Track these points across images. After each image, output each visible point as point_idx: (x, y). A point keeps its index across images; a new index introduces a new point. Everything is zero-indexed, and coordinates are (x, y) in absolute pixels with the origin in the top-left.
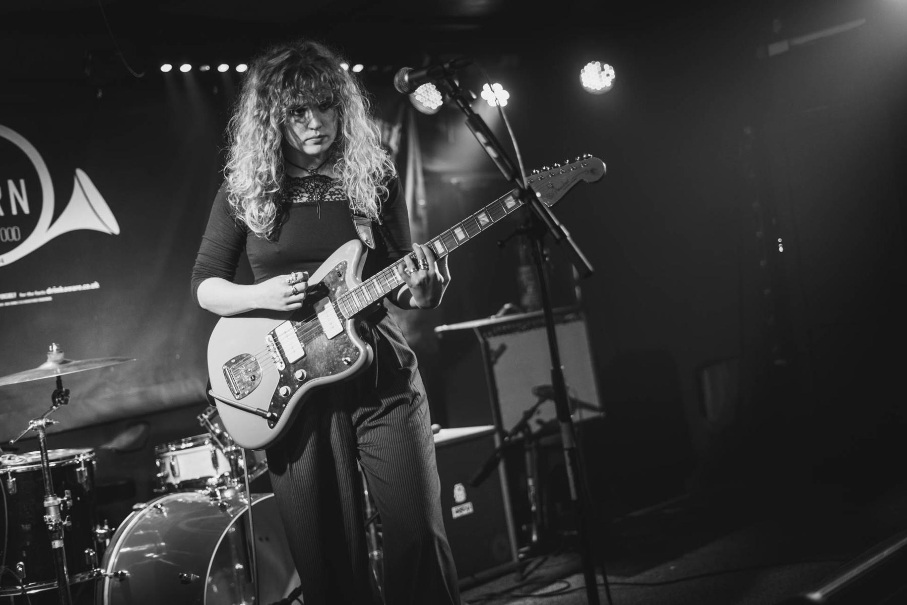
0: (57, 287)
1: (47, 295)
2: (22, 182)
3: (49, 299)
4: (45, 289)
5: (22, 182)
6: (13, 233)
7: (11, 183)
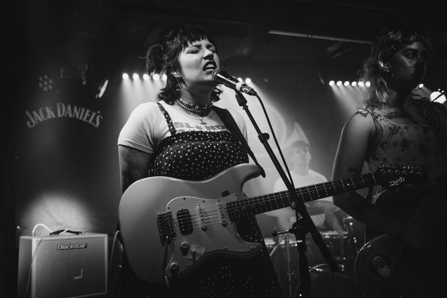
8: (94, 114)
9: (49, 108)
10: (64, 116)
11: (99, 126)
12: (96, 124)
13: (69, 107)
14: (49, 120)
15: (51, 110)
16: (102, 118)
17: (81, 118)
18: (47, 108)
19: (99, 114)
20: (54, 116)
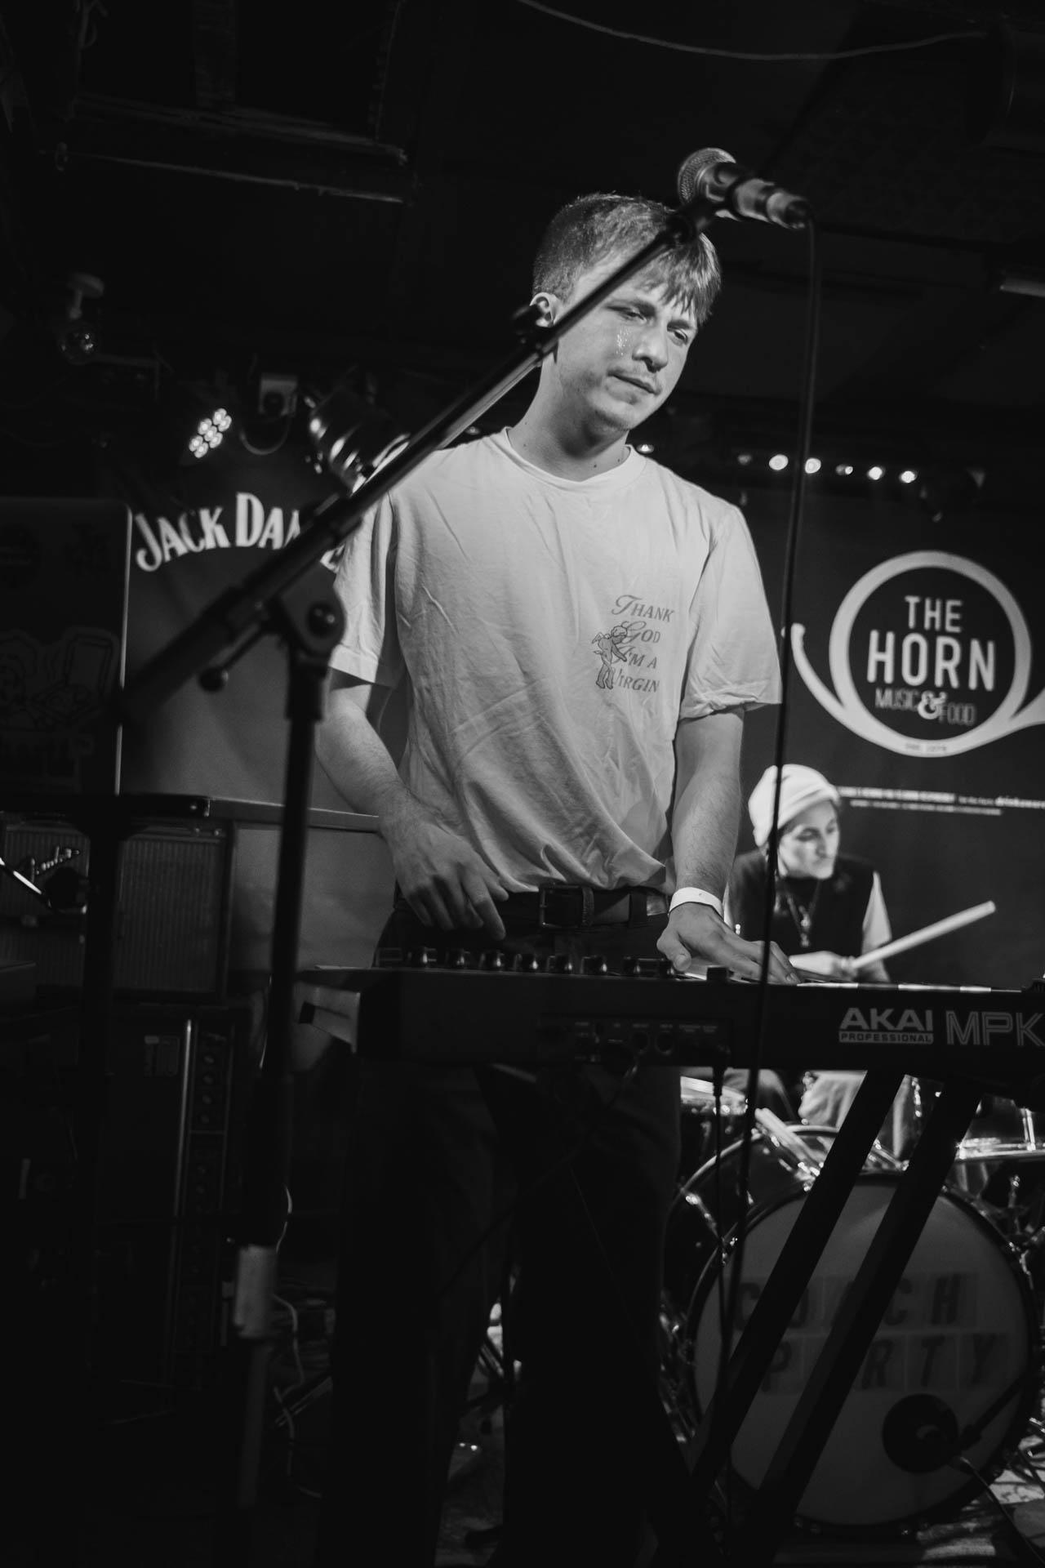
0: (1012, 797)
1: (995, 807)
2: (991, 646)
3: (997, 812)
4: (995, 797)
5: (991, 646)
6: (965, 713)
7: (975, 646)
9: (212, 514)
10: (256, 545)
13: (277, 515)
14: (205, 551)
15: (219, 522)
18: (204, 514)
20: (224, 542)
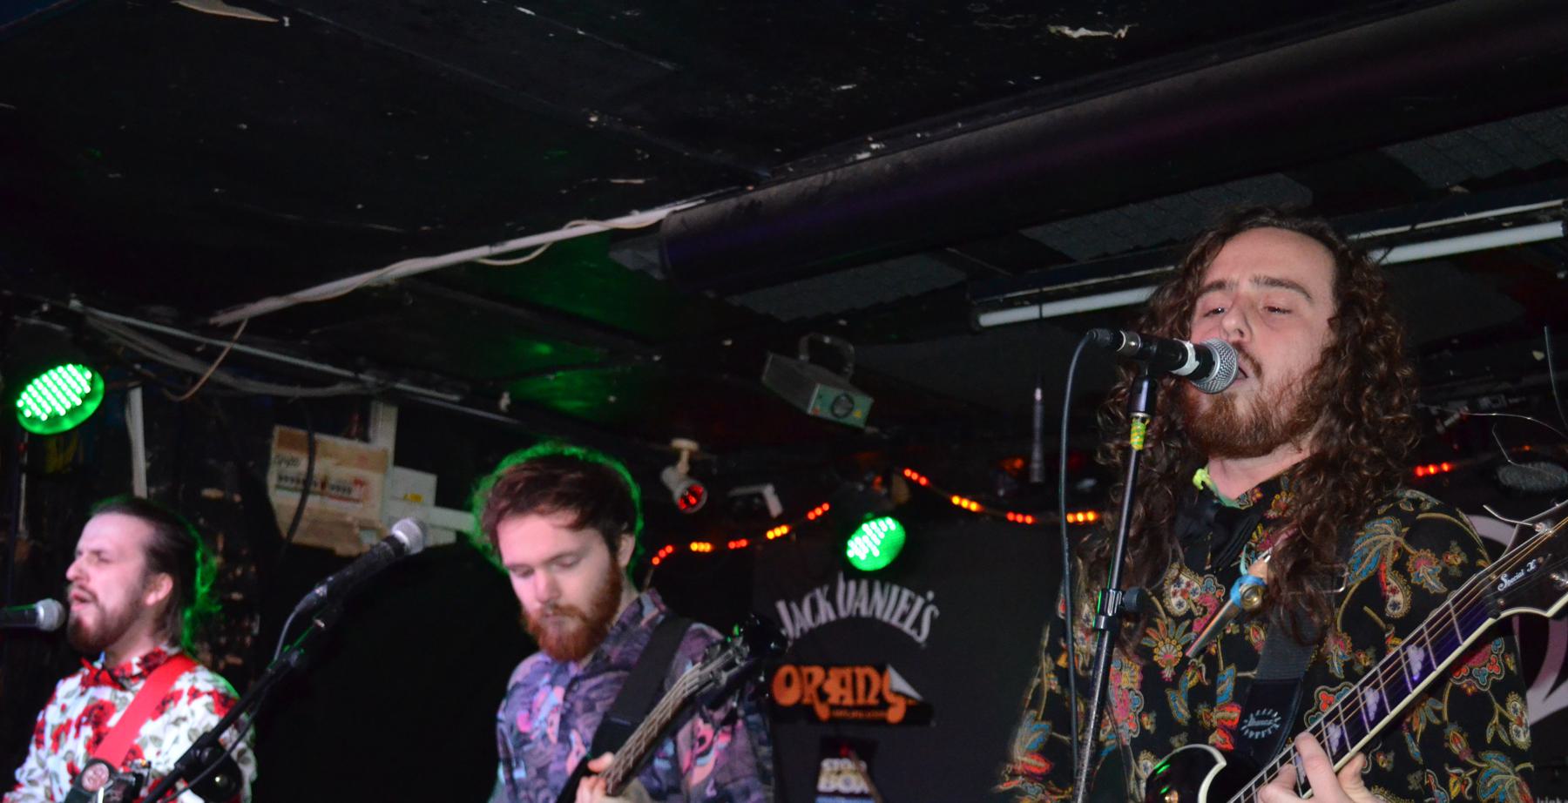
8: (920, 602)
11: (928, 640)
12: (919, 634)
14: (821, 627)
16: (937, 613)
17: (886, 618)
19: (934, 602)
20: (832, 617)
